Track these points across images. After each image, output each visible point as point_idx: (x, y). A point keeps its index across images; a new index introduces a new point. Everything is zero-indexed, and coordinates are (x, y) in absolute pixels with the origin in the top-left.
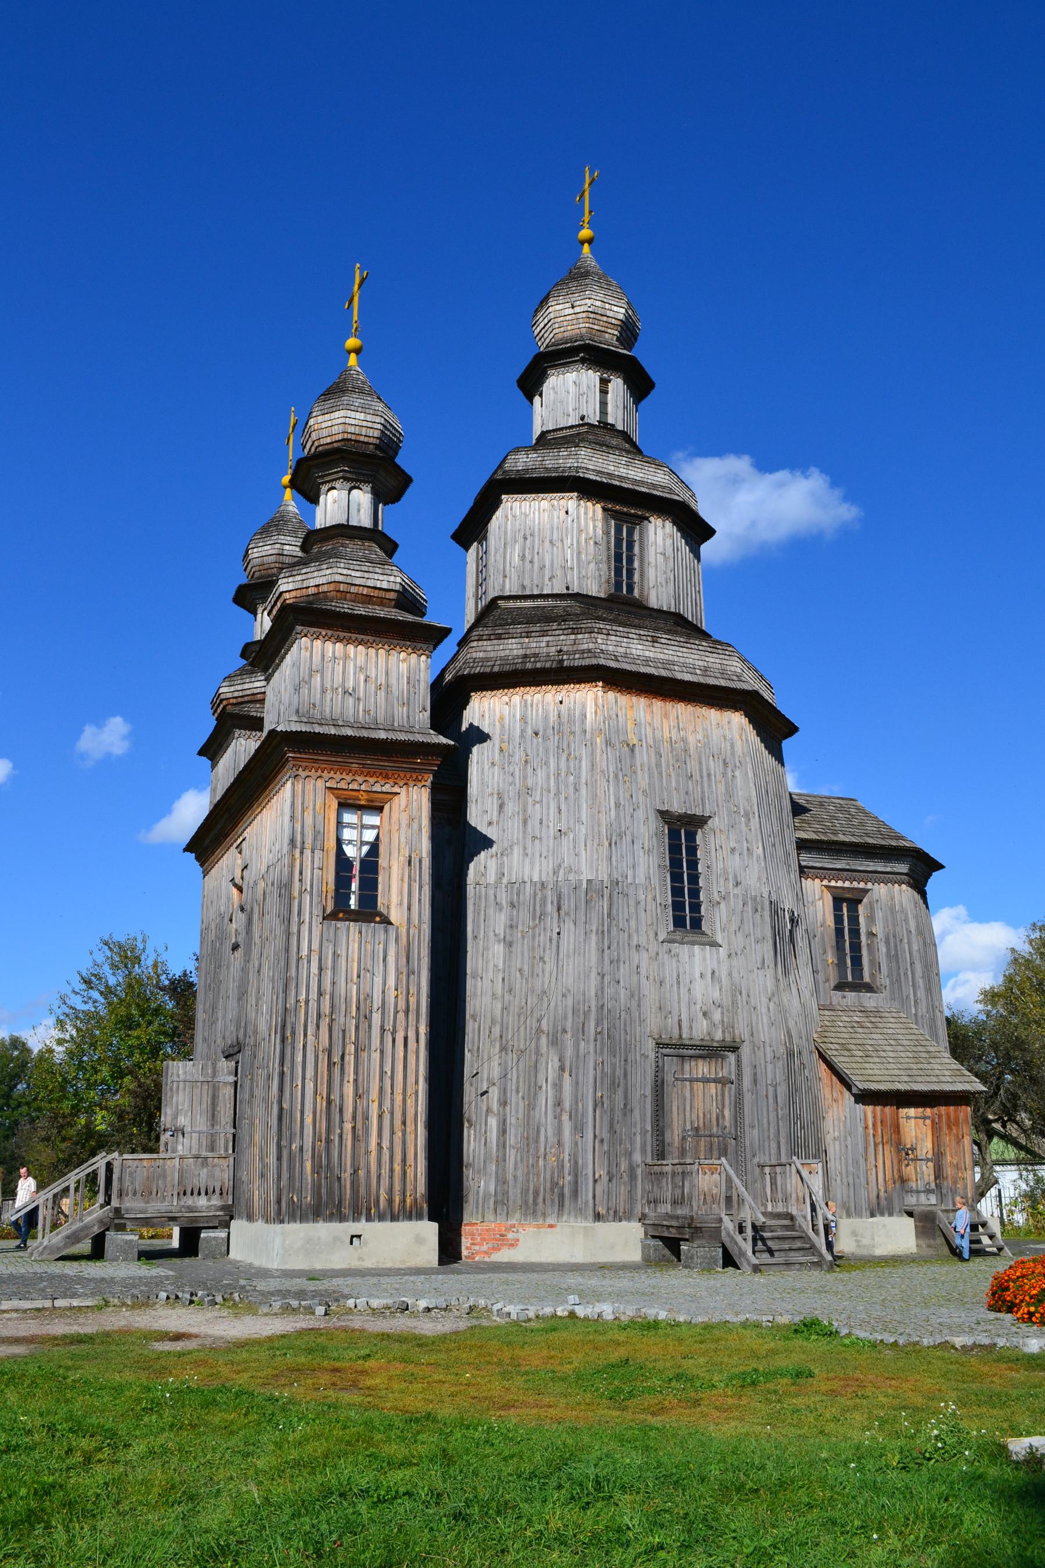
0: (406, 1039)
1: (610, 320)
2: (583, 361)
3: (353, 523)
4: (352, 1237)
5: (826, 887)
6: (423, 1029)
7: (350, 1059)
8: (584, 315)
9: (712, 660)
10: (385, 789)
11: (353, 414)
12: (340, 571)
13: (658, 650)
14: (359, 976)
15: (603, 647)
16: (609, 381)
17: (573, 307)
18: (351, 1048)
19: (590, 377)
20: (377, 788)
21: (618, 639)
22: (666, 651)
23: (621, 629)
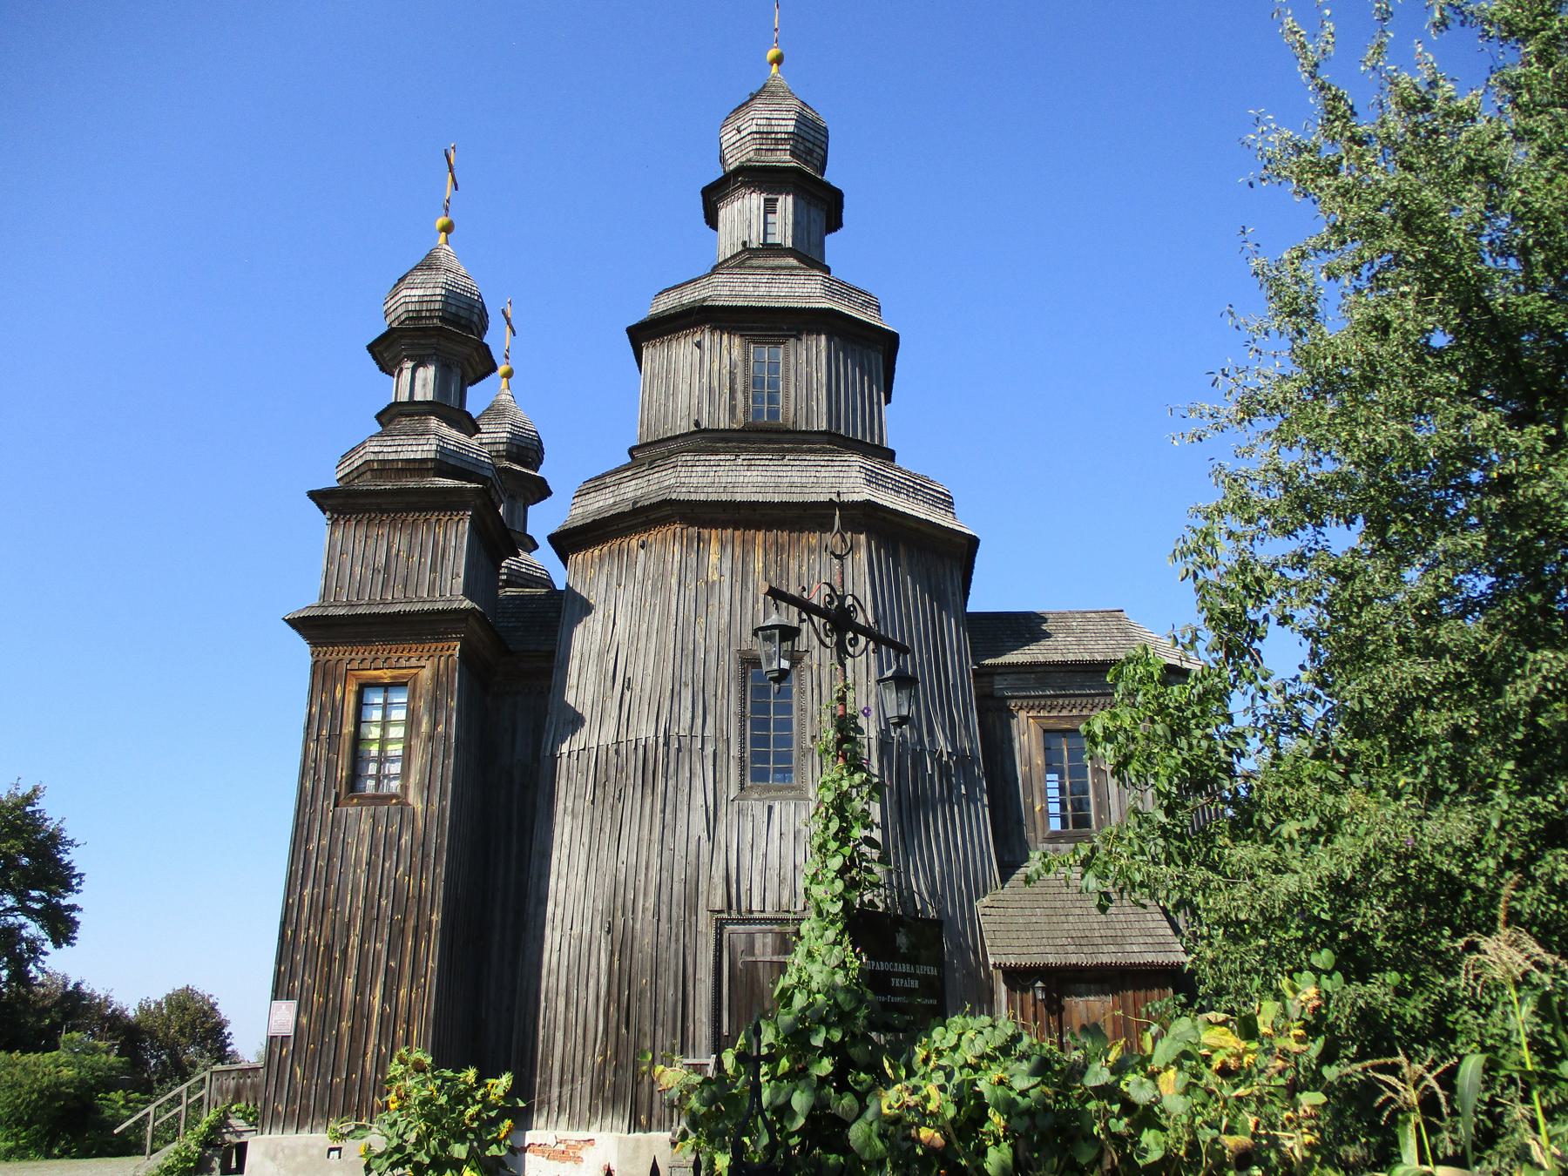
0: (416, 928)
1: (779, 136)
2: (744, 184)
3: (418, 397)
4: (331, 1150)
5: (1032, 717)
6: (436, 918)
7: (354, 954)
8: (749, 137)
9: (827, 474)
10: (413, 662)
11: (414, 292)
12: (372, 449)
13: (755, 473)
14: (368, 864)
15: (687, 480)
16: (777, 200)
17: (739, 132)
18: (355, 940)
19: (756, 200)
20: (403, 663)
21: (704, 469)
22: (764, 473)
23: (712, 458)
